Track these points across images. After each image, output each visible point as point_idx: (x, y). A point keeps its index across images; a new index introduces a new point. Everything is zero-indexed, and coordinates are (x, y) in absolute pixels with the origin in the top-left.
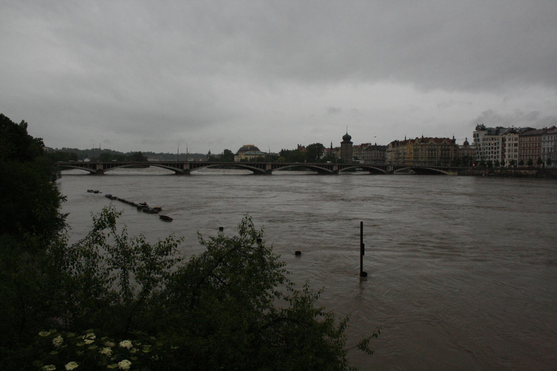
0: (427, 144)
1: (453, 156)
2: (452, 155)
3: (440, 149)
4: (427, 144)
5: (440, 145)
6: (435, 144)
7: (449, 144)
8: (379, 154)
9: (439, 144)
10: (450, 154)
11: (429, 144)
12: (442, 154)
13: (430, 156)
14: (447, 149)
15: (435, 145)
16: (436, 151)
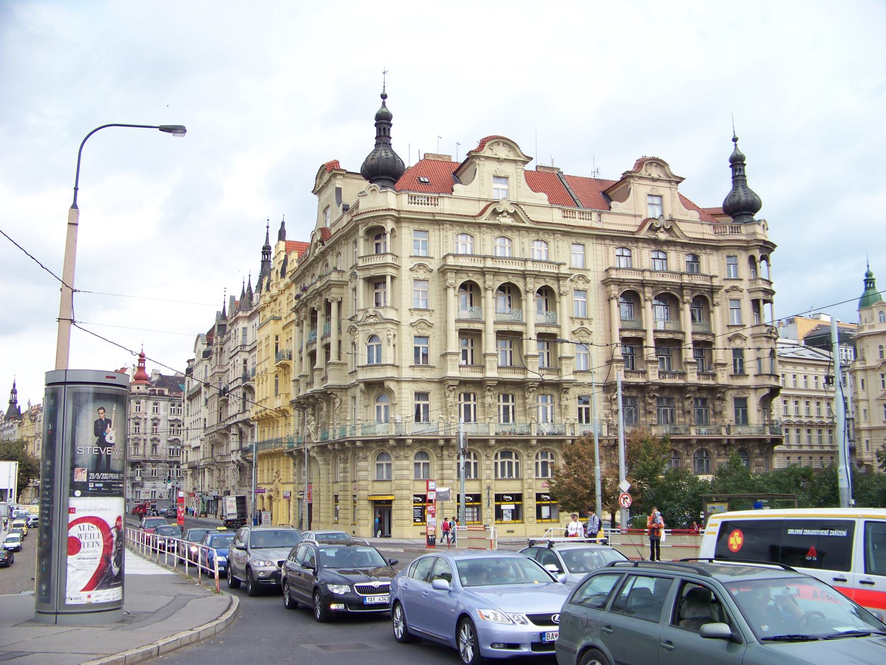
0: (446, 206)
1: (750, 367)
2: (738, 353)
3: (606, 283)
4: (446, 206)
5: (602, 237)
6: (537, 215)
7: (707, 232)
8: (163, 425)
9: (593, 222)
10: (722, 354)
11: (473, 209)
12: (633, 344)
13: (492, 373)
14: (694, 287)
15: (542, 230)
16: (566, 306)
